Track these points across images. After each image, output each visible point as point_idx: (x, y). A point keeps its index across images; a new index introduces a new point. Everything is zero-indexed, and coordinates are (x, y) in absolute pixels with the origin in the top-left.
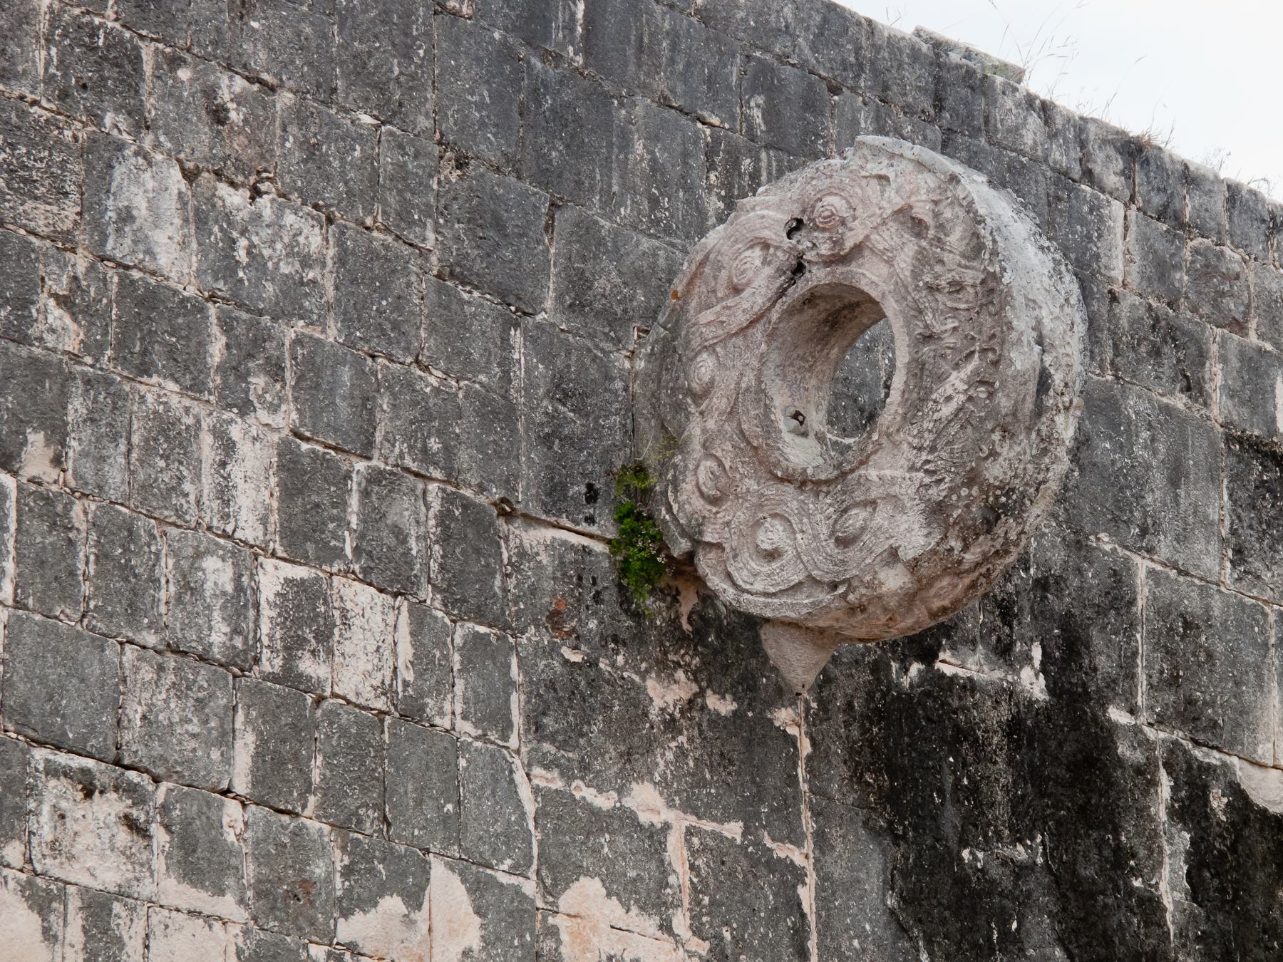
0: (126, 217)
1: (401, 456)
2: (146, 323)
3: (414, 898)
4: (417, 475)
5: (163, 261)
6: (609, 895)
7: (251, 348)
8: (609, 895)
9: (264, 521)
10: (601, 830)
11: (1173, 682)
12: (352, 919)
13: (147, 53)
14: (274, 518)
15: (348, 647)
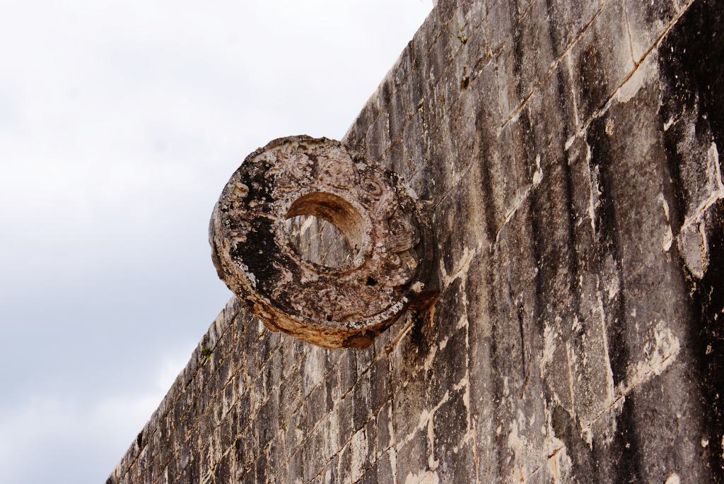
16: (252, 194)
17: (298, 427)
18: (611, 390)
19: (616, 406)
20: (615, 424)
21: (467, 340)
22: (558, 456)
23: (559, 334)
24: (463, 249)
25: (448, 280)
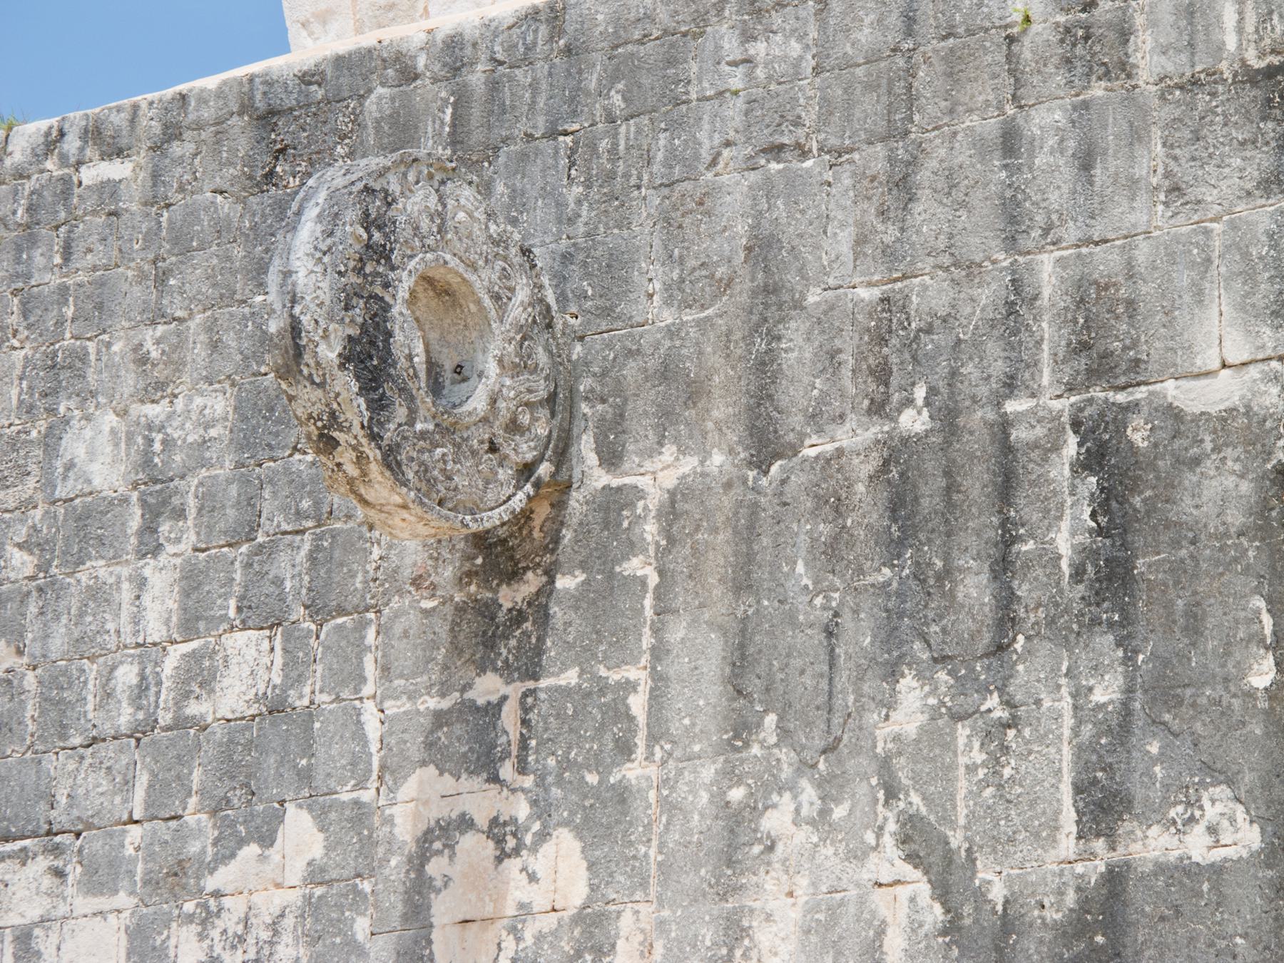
0: (70, 466)
1: (279, 526)
2: (86, 526)
3: (267, 840)
4: (297, 532)
5: (97, 482)
6: (441, 774)
7: (159, 508)
8: (441, 774)
9: (167, 622)
10: (441, 727)
11: (1085, 346)
12: (216, 874)
13: (91, 347)
14: (174, 619)
15: (226, 682)
18: (1067, 844)
19: (1079, 868)
20: (1071, 898)
22: (903, 892)
23: (943, 704)
24: (661, 444)
25: (601, 478)
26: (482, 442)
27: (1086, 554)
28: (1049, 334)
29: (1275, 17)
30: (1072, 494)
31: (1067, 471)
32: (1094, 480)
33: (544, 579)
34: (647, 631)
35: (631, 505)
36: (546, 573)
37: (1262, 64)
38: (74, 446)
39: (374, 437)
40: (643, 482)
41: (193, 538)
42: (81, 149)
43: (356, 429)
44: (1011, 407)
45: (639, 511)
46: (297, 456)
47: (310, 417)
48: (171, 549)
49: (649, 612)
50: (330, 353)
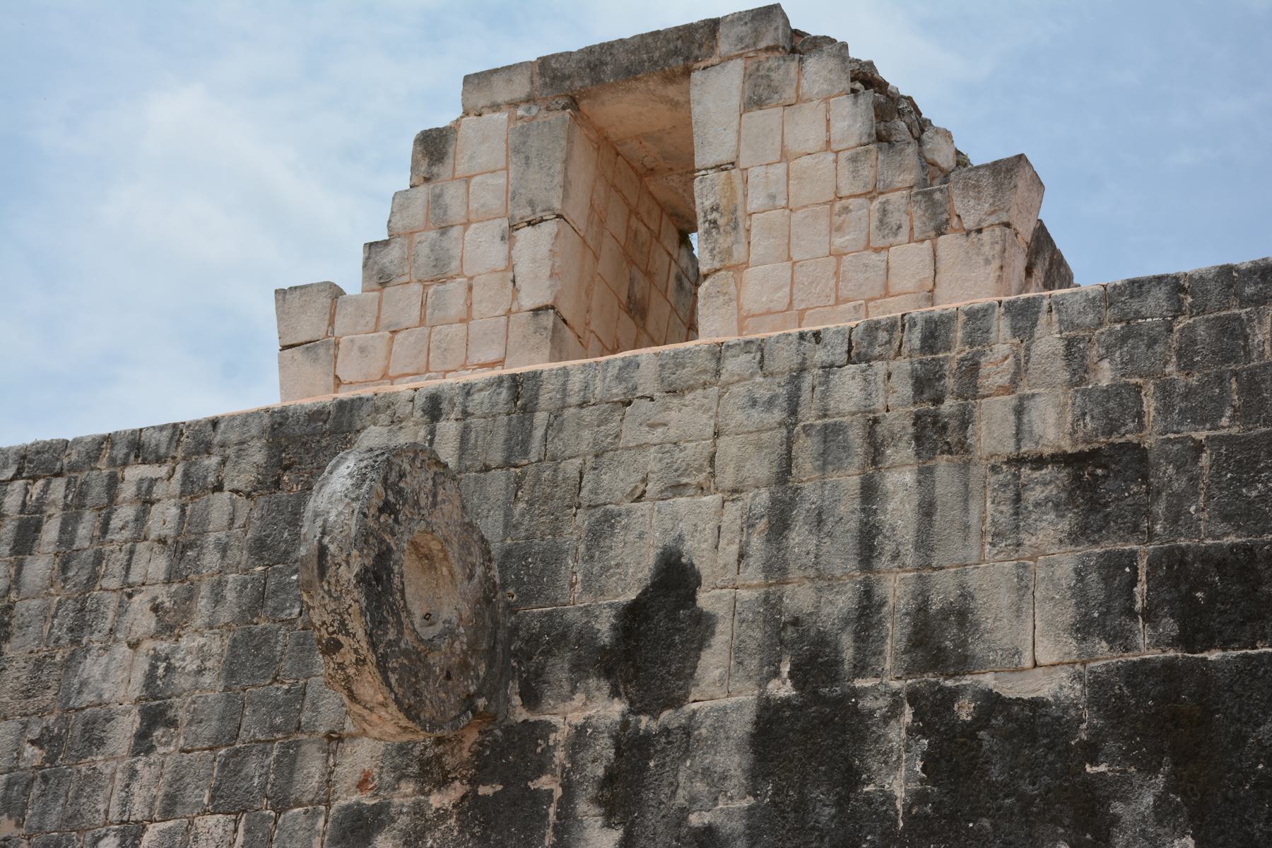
16: (386, 508)
17: (33, 742)
21: (552, 811)
24: (573, 692)
25: (521, 714)
26: (442, 670)
27: (919, 798)
28: (894, 634)
29: (1088, 418)
30: (906, 751)
31: (903, 735)
32: (926, 742)
33: (468, 787)
34: (549, 832)
35: (546, 739)
36: (469, 782)
37: (1074, 450)
38: (92, 668)
39: (373, 646)
40: (555, 720)
41: (182, 742)
42: (127, 455)
43: (360, 634)
44: (859, 683)
45: (551, 743)
46: (276, 685)
47: (324, 623)
48: (161, 750)
49: (552, 818)
50: (348, 574)
